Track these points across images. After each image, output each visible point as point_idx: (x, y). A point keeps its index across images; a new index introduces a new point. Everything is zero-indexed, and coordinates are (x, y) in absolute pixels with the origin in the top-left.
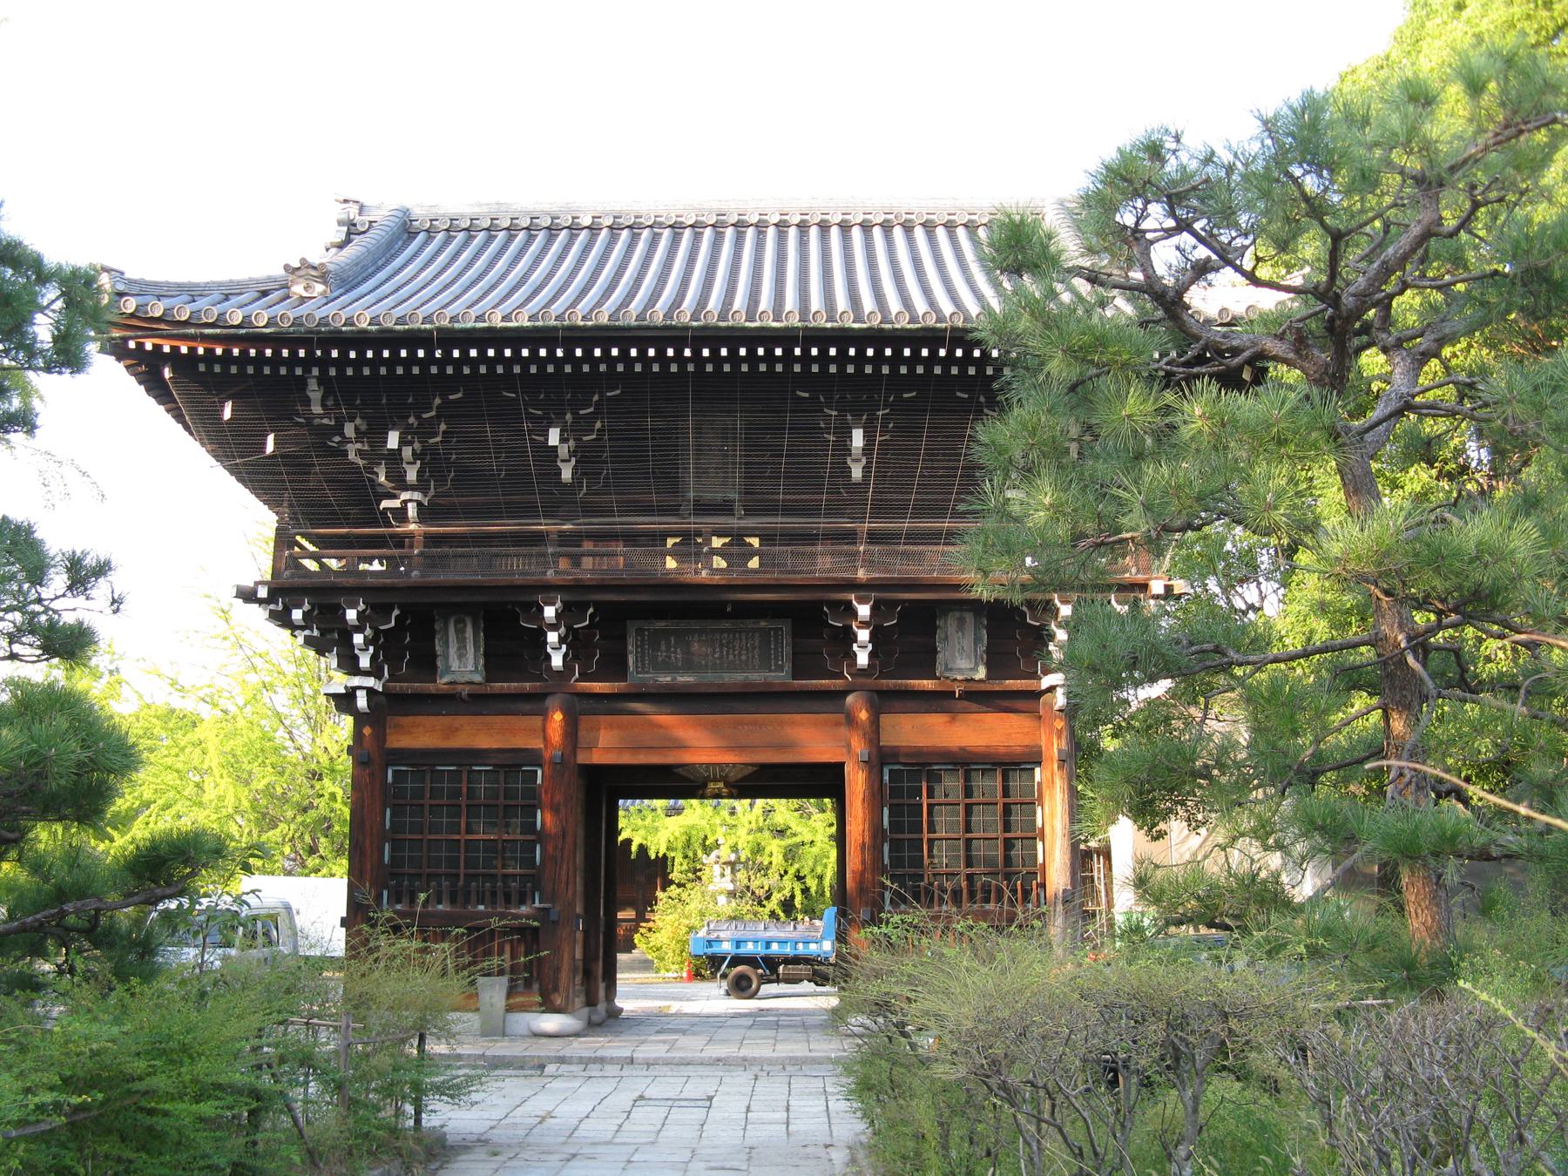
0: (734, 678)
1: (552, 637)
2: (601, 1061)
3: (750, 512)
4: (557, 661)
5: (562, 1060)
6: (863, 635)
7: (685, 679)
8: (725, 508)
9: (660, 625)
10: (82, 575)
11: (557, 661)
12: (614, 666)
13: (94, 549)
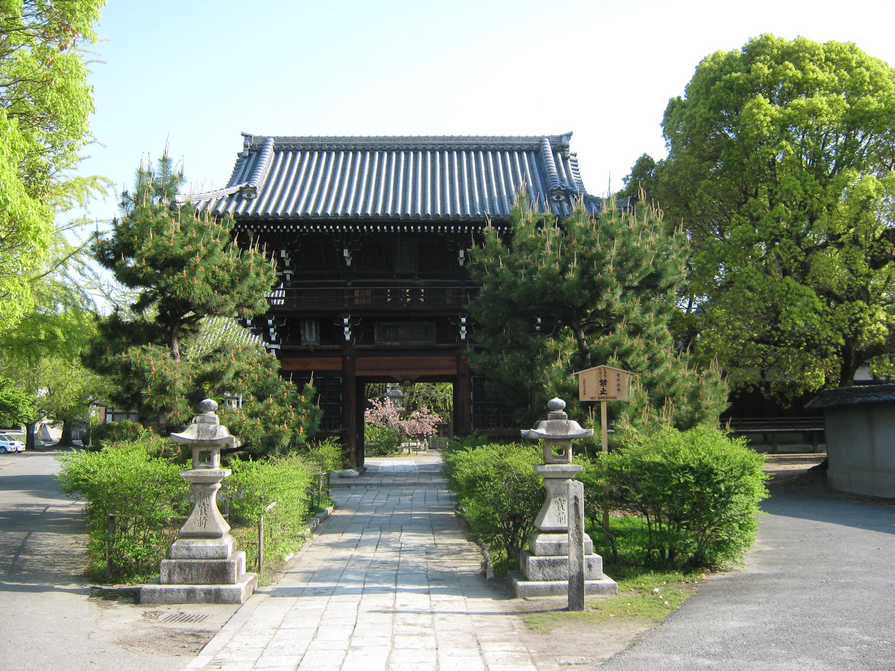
0: (415, 343)
1: (347, 329)
2: (371, 485)
3: (420, 277)
4: (348, 337)
5: (357, 485)
6: (463, 328)
7: (396, 344)
8: (410, 276)
9: (387, 323)
10: (575, 155)
11: (348, 337)
12: (370, 338)
13: (567, 131)
